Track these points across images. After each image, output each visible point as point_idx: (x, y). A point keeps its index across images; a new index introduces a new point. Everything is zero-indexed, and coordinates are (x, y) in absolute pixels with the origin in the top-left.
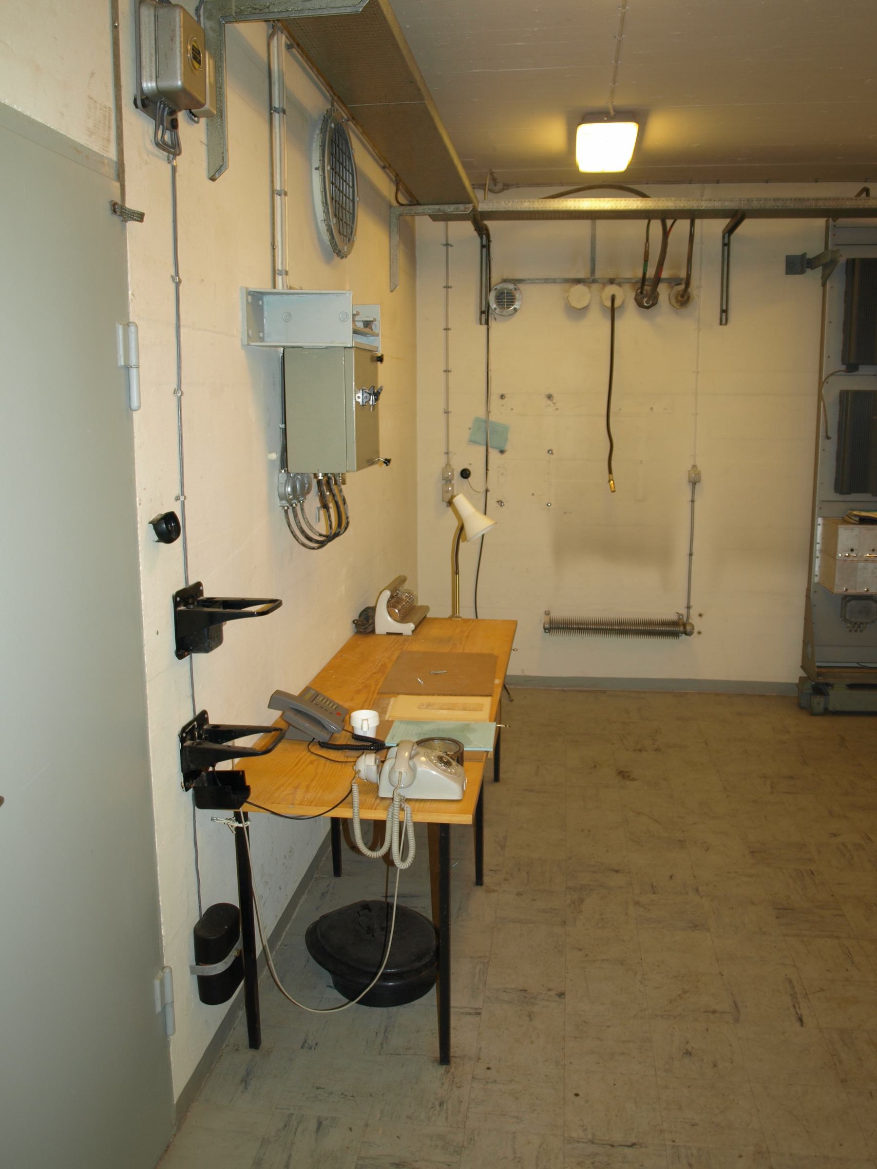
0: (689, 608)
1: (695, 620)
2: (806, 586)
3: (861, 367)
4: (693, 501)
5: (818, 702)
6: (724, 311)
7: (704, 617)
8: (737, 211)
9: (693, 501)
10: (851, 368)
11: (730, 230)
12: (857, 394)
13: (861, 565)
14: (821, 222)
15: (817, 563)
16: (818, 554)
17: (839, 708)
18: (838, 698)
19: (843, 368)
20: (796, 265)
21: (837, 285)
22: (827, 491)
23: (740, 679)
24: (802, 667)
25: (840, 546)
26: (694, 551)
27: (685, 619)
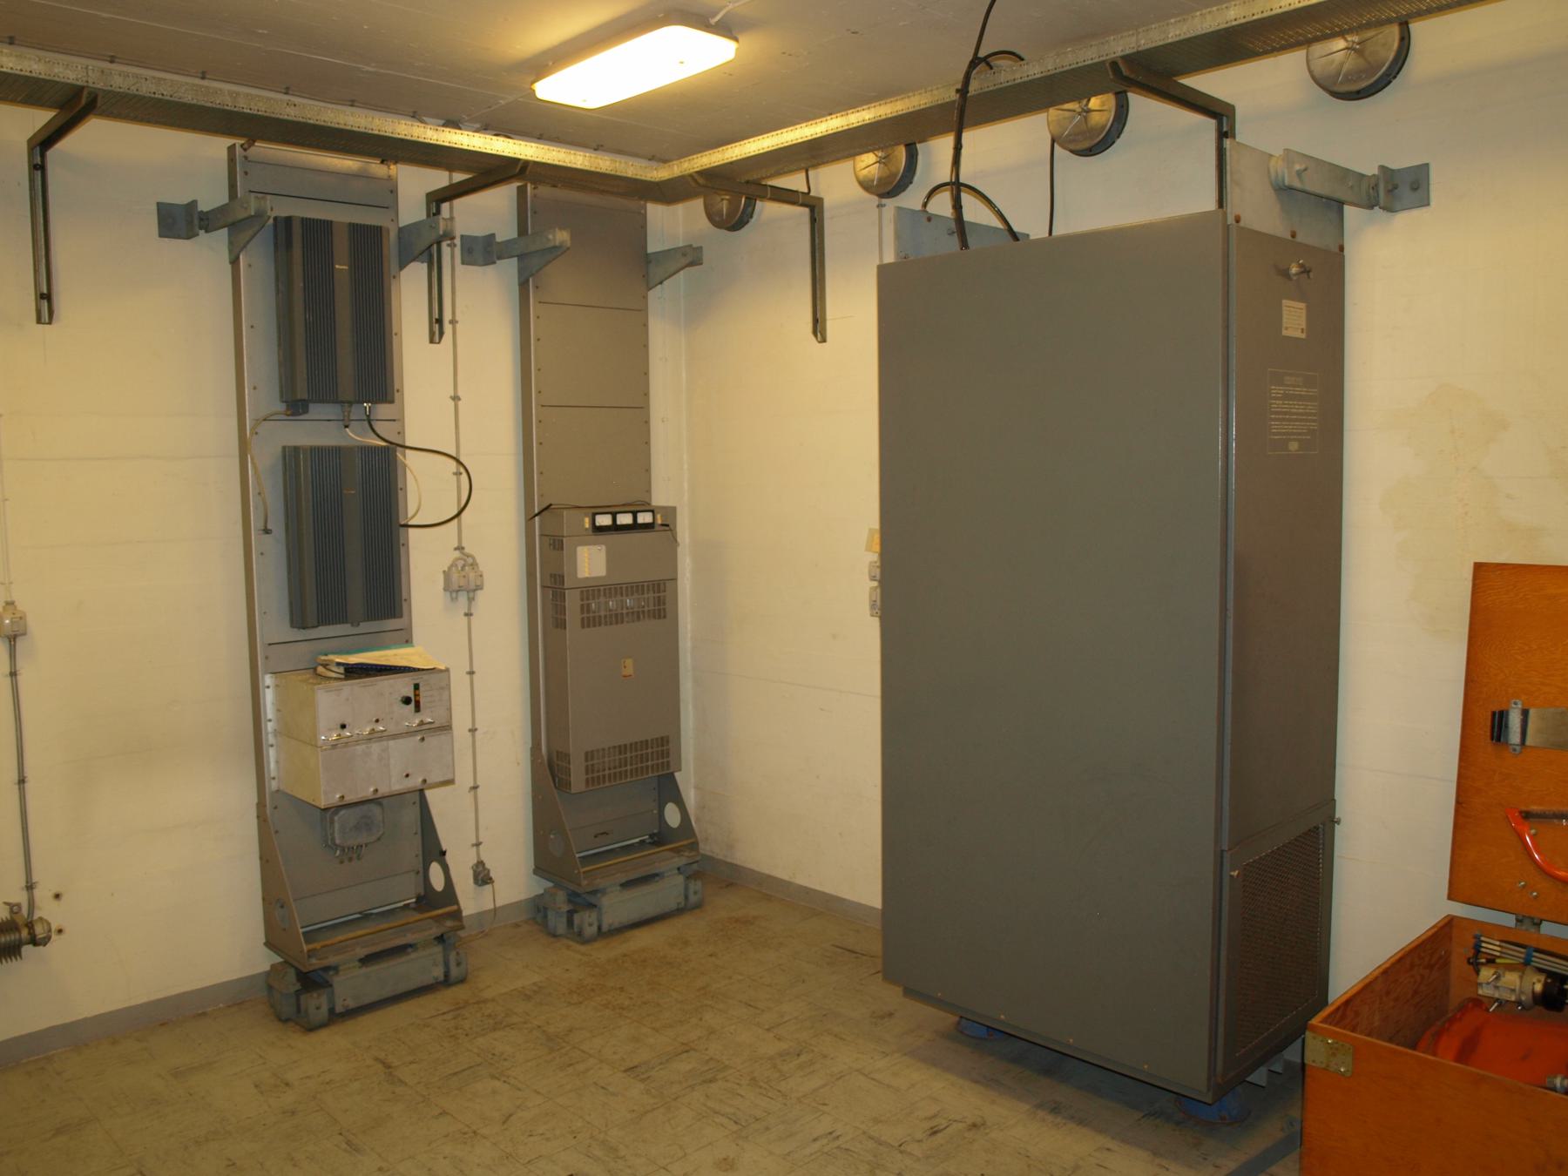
0: (30, 887)
1: (47, 910)
2: (253, 798)
3: (311, 406)
4: (13, 674)
5: (316, 1004)
6: (46, 297)
7: (64, 898)
8: (77, 91)
9: (13, 674)
10: (296, 407)
11: (45, 142)
12: (318, 453)
13: (360, 748)
14: (215, 148)
15: (272, 755)
16: (271, 740)
17: (352, 1004)
18: (350, 986)
19: (281, 407)
20: (178, 222)
21: (258, 262)
22: (276, 626)
23: (153, 998)
24: (268, 944)
25: (322, 724)
26: (29, 773)
27: (25, 911)
